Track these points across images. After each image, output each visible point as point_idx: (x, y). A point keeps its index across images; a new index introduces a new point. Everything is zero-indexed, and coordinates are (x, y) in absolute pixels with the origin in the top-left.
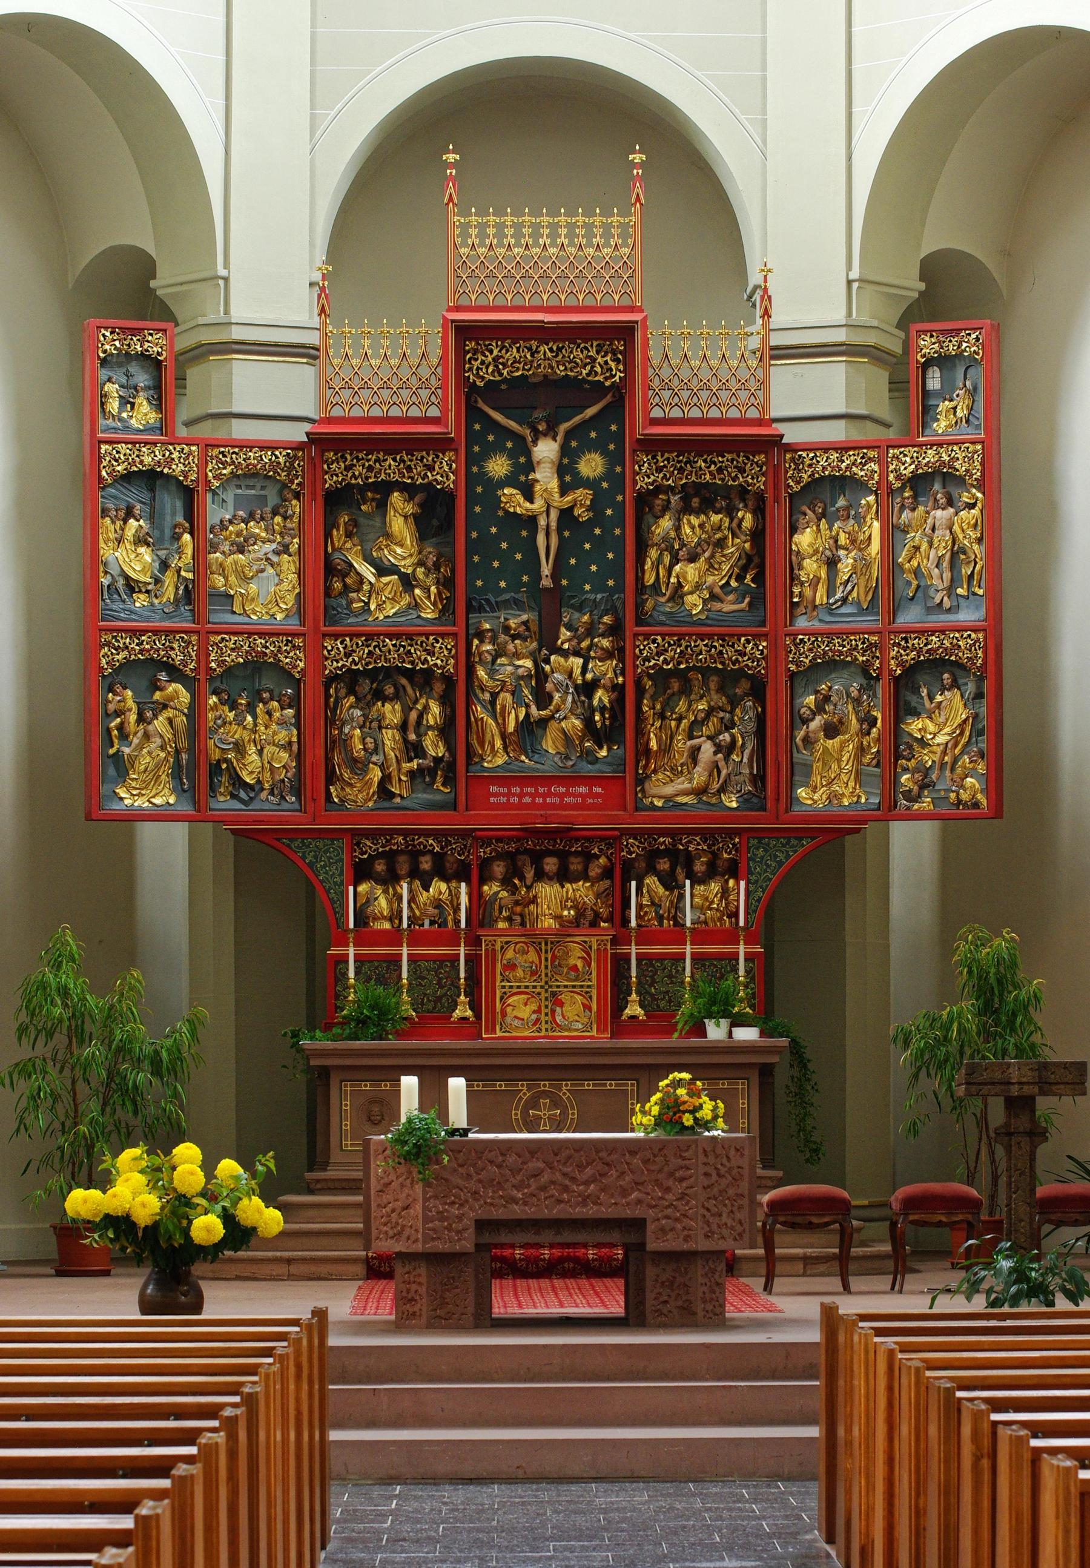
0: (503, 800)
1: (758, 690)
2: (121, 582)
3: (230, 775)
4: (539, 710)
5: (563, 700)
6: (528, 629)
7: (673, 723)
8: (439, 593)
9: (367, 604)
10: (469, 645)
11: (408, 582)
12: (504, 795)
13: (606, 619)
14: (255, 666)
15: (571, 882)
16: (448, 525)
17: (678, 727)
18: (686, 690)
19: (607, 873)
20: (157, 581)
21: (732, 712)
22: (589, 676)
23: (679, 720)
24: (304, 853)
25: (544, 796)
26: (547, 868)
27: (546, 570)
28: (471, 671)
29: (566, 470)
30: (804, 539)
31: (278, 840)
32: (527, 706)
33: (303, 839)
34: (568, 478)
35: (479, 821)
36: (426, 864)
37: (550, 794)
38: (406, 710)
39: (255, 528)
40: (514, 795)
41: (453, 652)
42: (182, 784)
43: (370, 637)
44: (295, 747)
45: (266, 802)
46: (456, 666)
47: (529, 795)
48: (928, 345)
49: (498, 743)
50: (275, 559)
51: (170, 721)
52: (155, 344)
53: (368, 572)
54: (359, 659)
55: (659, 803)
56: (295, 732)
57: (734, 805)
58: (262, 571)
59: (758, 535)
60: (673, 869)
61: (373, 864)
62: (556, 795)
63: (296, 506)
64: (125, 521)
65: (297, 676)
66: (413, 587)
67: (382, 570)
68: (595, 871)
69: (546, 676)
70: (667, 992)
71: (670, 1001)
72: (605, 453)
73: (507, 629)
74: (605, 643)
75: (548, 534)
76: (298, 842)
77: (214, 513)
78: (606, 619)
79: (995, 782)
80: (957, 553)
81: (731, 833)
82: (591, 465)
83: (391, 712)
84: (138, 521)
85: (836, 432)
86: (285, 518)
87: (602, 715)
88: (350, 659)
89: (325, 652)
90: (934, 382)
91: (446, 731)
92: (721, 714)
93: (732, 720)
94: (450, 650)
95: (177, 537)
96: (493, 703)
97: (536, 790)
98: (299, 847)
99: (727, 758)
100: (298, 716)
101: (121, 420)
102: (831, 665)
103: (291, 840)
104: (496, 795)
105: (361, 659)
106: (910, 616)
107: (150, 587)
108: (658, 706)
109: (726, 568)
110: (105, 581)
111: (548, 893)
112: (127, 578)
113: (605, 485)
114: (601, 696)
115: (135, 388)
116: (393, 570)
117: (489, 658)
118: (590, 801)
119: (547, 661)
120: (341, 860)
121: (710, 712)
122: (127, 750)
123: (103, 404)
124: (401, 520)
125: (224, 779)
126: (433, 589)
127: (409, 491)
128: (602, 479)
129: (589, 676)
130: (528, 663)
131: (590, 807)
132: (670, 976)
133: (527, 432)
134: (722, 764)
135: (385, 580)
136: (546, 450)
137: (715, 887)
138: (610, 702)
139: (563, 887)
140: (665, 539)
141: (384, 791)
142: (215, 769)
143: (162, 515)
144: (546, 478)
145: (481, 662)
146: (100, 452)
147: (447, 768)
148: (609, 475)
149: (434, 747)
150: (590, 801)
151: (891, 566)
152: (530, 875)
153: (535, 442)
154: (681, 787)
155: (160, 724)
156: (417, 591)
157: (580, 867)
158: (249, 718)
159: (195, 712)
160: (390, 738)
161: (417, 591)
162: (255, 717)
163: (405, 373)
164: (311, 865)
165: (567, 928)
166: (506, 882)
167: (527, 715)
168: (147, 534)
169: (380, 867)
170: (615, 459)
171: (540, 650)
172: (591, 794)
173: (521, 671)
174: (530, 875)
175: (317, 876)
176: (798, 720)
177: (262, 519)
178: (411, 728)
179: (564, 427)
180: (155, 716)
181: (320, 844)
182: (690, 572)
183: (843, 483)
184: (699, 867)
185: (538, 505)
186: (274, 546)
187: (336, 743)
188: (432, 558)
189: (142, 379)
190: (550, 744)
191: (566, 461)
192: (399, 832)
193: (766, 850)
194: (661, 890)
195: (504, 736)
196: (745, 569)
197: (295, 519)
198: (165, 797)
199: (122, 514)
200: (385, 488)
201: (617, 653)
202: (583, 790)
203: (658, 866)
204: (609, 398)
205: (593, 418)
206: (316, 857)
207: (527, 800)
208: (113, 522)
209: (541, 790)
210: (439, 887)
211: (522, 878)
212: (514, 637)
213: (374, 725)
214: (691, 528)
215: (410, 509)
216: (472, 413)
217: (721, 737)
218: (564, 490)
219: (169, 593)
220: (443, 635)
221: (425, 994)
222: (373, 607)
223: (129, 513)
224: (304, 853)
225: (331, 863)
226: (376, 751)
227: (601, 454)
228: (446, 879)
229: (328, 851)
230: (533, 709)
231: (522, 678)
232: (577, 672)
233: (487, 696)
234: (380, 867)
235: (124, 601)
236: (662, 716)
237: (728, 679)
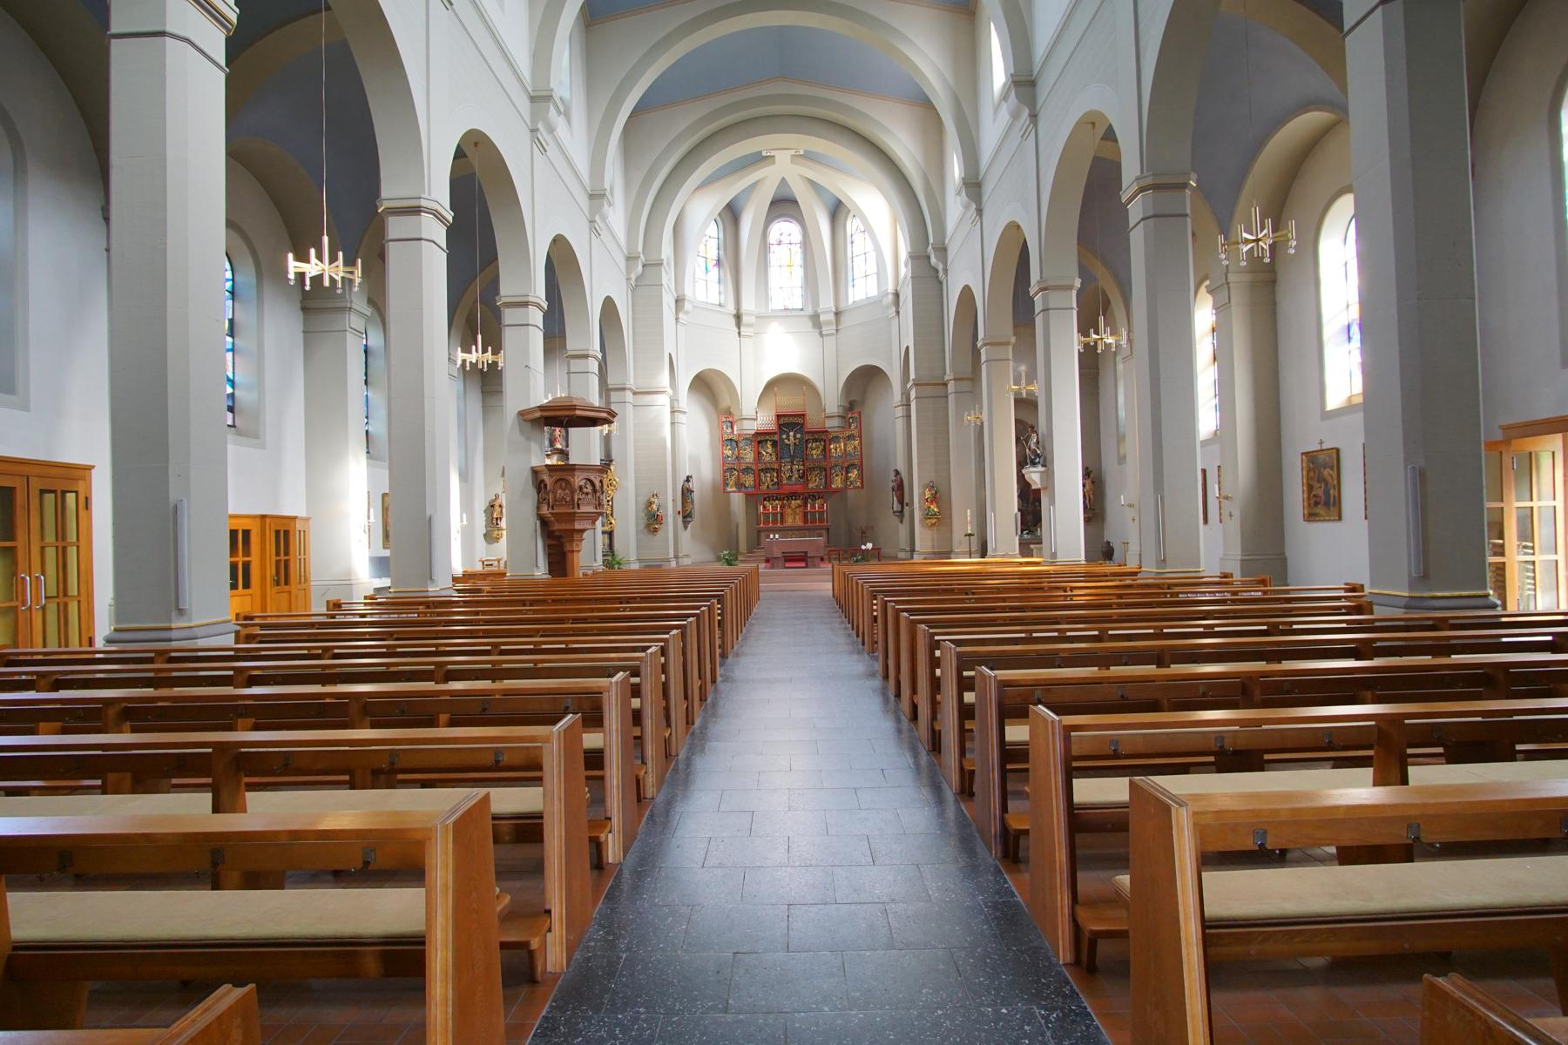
1: (825, 470)
5: (795, 472)
11: (771, 455)
14: (748, 468)
16: (776, 446)
29: (794, 436)
30: (832, 446)
35: (783, 492)
45: (750, 489)
48: (850, 415)
52: (731, 419)
53: (764, 453)
54: (764, 467)
59: (824, 446)
67: (767, 453)
77: (741, 445)
79: (862, 482)
80: (855, 447)
83: (768, 475)
85: (836, 429)
90: (851, 421)
91: (777, 478)
102: (837, 465)
106: (848, 458)
111: (793, 502)
114: (801, 471)
136: (792, 434)
141: (768, 487)
144: (792, 438)
149: (775, 480)
151: (845, 450)
159: (739, 475)
160: (768, 479)
165: (797, 507)
176: (831, 474)
182: (814, 452)
183: (837, 437)
187: (760, 480)
189: (729, 424)
190: (793, 479)
198: (734, 489)
200: (767, 440)
201: (803, 465)
210: (777, 502)
213: (766, 477)
214: (814, 445)
216: (780, 428)
237: (820, 468)
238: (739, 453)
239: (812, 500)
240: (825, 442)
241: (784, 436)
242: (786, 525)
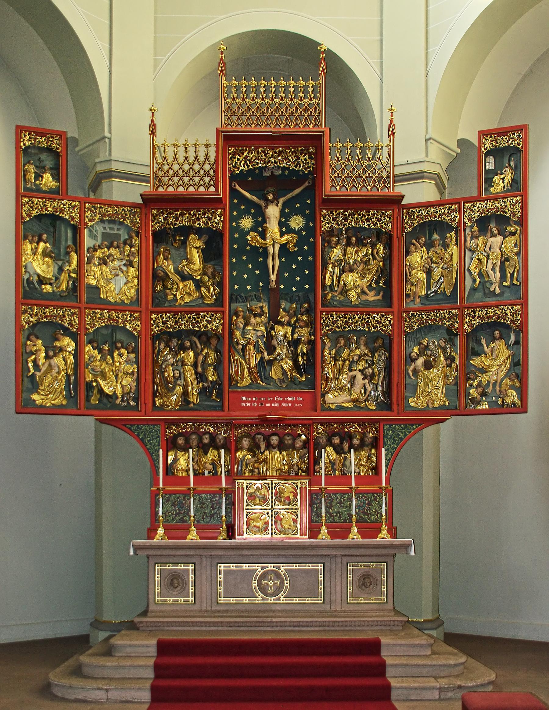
0: (248, 404)
2: (36, 278)
3: (99, 389)
4: (268, 355)
6: (263, 311)
7: (341, 363)
8: (214, 290)
9: (175, 296)
10: (230, 319)
11: (198, 285)
12: (249, 402)
13: (305, 305)
15: (285, 451)
17: (343, 365)
18: (347, 345)
19: (306, 444)
20: (57, 279)
21: (372, 357)
22: (296, 336)
23: (344, 361)
24: (138, 433)
25: (271, 402)
26: (272, 442)
27: (273, 278)
28: (232, 334)
29: (284, 225)
31: (125, 425)
32: (262, 353)
33: (138, 425)
34: (284, 229)
35: (236, 416)
36: (206, 440)
37: (274, 401)
38: (196, 355)
39: (112, 251)
40: (254, 402)
41: (222, 321)
42: (71, 393)
43: (176, 313)
46: (223, 330)
47: (263, 402)
49: (246, 372)
50: (124, 269)
51: (64, 359)
55: (333, 407)
57: (374, 408)
58: (117, 275)
60: (341, 442)
61: (177, 439)
62: (277, 402)
63: (135, 240)
64: (38, 243)
65: (136, 334)
66: (200, 287)
68: (298, 444)
69: (272, 337)
70: (339, 512)
71: (340, 517)
72: (304, 215)
73: (251, 310)
74: (305, 318)
75: (273, 258)
76: (135, 427)
78: (305, 305)
81: (373, 422)
82: (297, 222)
84: (45, 243)
86: (131, 247)
87: (303, 358)
88: (166, 326)
89: (152, 321)
92: (367, 358)
93: (372, 361)
94: (220, 321)
95: (68, 253)
96: (244, 350)
97: (267, 399)
98: (136, 430)
99: (370, 382)
101: (35, 185)
103: (132, 425)
104: (245, 402)
105: (171, 326)
107: (52, 281)
108: (333, 353)
109: (369, 277)
110: (26, 277)
112: (39, 276)
113: (304, 233)
115: (44, 168)
116: (190, 277)
117: (241, 326)
118: (296, 405)
119: (273, 328)
120: (159, 437)
121: (360, 357)
122: (38, 374)
123: (25, 176)
124: (195, 249)
125: (95, 392)
126: (212, 289)
127: (199, 232)
128: (302, 230)
129: (296, 336)
130: (263, 329)
131: (297, 409)
132: (340, 503)
133: (262, 203)
134: (367, 386)
135: (186, 283)
137: (364, 454)
138: (307, 351)
139: (281, 453)
140: (337, 261)
142: (89, 386)
143: (60, 241)
144: (273, 227)
145: (238, 328)
146: (22, 202)
147: (218, 385)
148: (306, 227)
150: (296, 405)
152: (263, 447)
153: (266, 207)
154: (345, 398)
155: (58, 361)
156: (202, 289)
157: (290, 442)
158: (109, 357)
159: (78, 353)
161: (202, 289)
162: (113, 358)
163: (197, 167)
166: (249, 450)
167: (262, 358)
168: (51, 251)
169: (181, 441)
170: (311, 218)
171: (269, 323)
172: (296, 401)
173: (259, 333)
174: (263, 447)
177: (118, 247)
178: (199, 365)
179: (281, 200)
180: (55, 355)
184: (356, 442)
185: (269, 242)
186: (124, 262)
188: (210, 271)
189: (49, 162)
190: (275, 373)
191: (283, 220)
192: (190, 420)
193: (393, 432)
194: (335, 455)
195: (249, 369)
196: (379, 278)
199: (36, 239)
200: (186, 231)
202: (292, 399)
203: (333, 441)
204: (306, 184)
205: (298, 195)
206: (145, 435)
207: (261, 405)
208: (31, 243)
209: (269, 399)
211: (259, 448)
212: (255, 315)
215: (198, 244)
216: (233, 191)
217: (367, 370)
218: (282, 235)
219: (64, 287)
220: (216, 312)
221: (205, 513)
222: (178, 297)
223: (40, 240)
224: (138, 433)
225: (153, 439)
226: (180, 377)
227: (302, 216)
228: (217, 448)
229: (151, 432)
230: (265, 354)
231: (258, 337)
232: (289, 334)
233: (241, 347)
234: (181, 441)
235: (37, 289)
236: (335, 359)
238: (79, 269)
239: (338, 450)
240: (389, 246)
241: (246, 223)
242: (238, 540)
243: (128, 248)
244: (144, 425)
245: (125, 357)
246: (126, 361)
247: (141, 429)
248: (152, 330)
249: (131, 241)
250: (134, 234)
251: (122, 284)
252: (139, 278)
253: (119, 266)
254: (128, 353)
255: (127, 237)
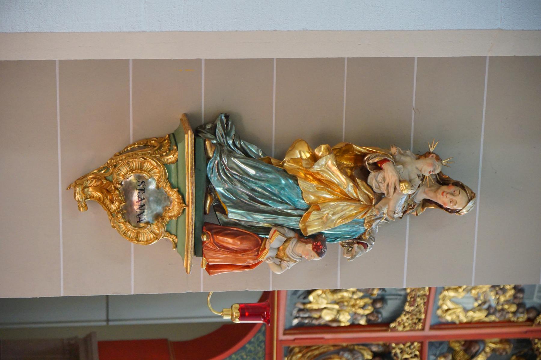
33: (264, 342)
44: (334, 325)
50: (486, 306)
56: (348, 324)
63: (523, 318)
65: (392, 325)
76: (262, 338)
86: (514, 313)
98: (258, 339)
100: (360, 325)
103: (264, 334)
164: (244, 348)
175: (235, 353)
181: (261, 354)
197: (512, 319)
206: (250, 351)
224: (253, 343)
243: (513, 308)
244: (265, 349)
245: (361, 311)
246: (355, 313)
247: (259, 345)
248: (397, 344)
249: (523, 313)
250: (531, 315)
251: (466, 306)
252: (470, 324)
253: (489, 301)
254: (367, 316)
255: (528, 306)
